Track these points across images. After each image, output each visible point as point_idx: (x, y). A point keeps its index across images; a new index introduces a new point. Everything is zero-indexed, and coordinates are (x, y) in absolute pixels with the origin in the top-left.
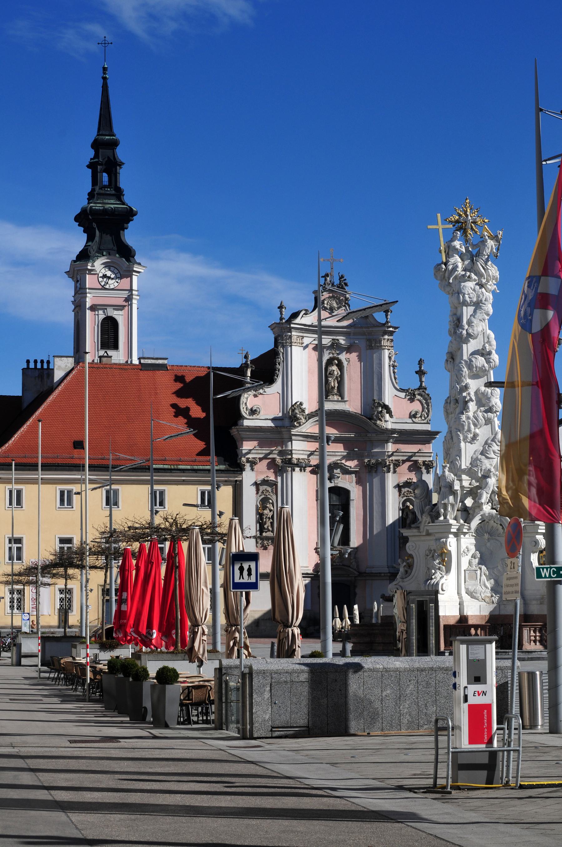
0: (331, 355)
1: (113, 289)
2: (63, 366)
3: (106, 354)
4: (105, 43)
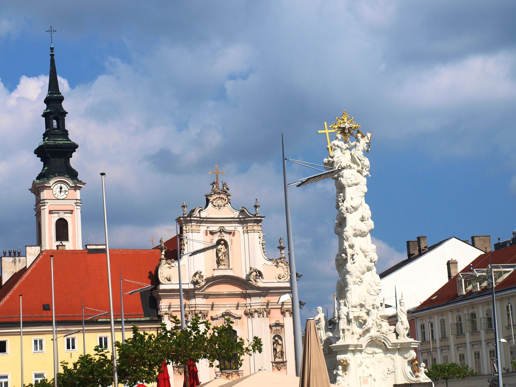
0: (220, 238)
1: (63, 199)
2: (33, 253)
3: (61, 244)
4: (51, 31)
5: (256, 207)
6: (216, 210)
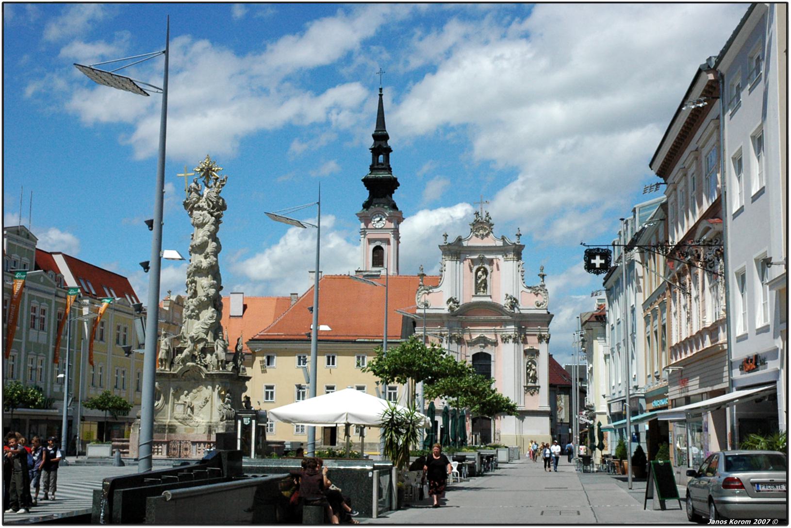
1: (381, 228)
5: (519, 236)
6: (479, 239)
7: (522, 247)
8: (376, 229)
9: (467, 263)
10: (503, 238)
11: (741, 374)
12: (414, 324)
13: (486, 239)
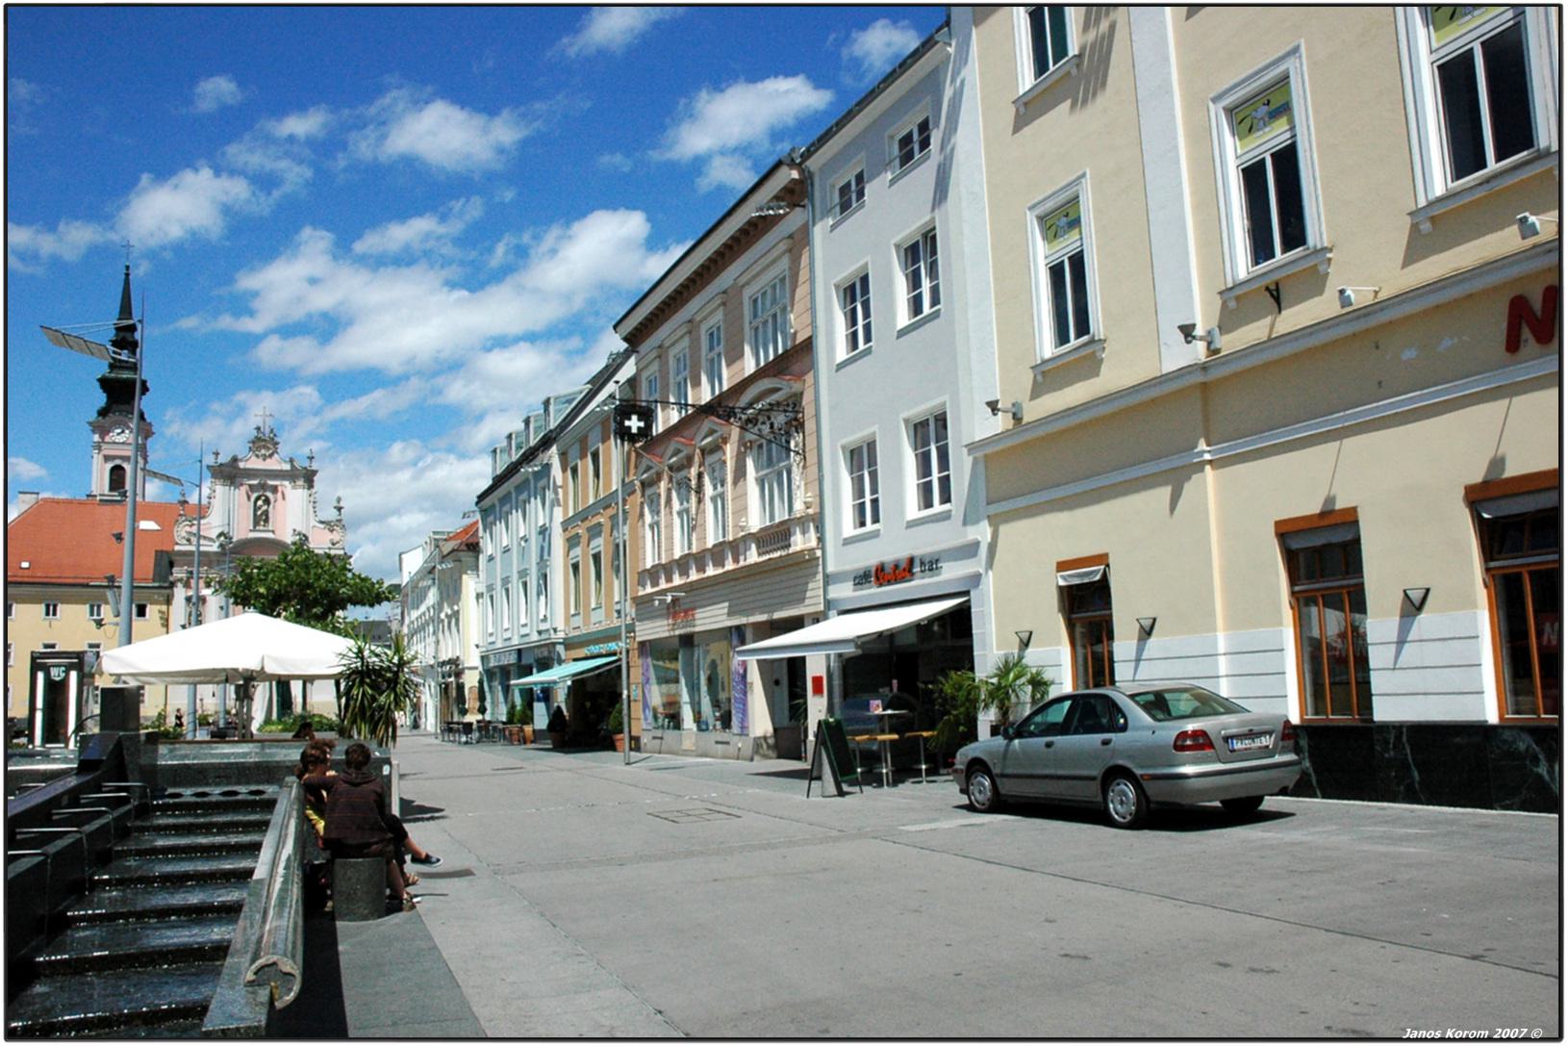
1: (123, 443)
6: (261, 460)
7: (314, 473)
8: (115, 443)
9: (244, 489)
10: (291, 461)
11: (854, 590)
12: (172, 564)
13: (268, 460)
